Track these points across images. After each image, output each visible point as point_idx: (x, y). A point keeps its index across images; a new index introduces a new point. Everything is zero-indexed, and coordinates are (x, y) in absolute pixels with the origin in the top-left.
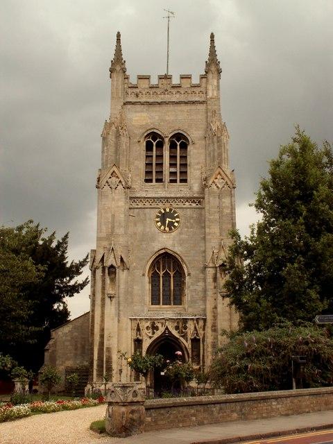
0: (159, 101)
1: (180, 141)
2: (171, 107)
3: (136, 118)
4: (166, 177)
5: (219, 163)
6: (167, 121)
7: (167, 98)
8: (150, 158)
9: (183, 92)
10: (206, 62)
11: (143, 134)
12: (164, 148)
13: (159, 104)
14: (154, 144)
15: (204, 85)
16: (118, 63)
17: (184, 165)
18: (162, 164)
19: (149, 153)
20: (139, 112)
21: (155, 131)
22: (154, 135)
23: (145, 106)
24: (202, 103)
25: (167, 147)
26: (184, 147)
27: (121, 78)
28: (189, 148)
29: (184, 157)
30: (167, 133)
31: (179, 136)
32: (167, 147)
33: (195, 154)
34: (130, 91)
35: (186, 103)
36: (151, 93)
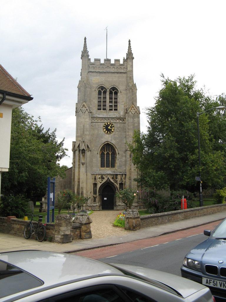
0: (105, 71)
1: (114, 91)
2: (110, 75)
3: (94, 79)
4: (108, 108)
5: (132, 102)
6: (109, 81)
7: (108, 70)
8: (100, 99)
9: (116, 68)
10: (82, 51)
11: (97, 87)
12: (107, 93)
13: (105, 73)
14: (102, 92)
15: (125, 65)
16: (85, 54)
17: (116, 102)
18: (106, 101)
19: (100, 96)
20: (95, 76)
21: (103, 86)
22: (102, 88)
23: (98, 74)
24: (125, 73)
25: (108, 93)
26: (116, 93)
27: (87, 60)
28: (118, 94)
29: (116, 99)
30: (108, 87)
31: (114, 89)
32: (108, 93)
33: (122, 98)
34: (91, 66)
35: (117, 73)
36: (101, 67)
